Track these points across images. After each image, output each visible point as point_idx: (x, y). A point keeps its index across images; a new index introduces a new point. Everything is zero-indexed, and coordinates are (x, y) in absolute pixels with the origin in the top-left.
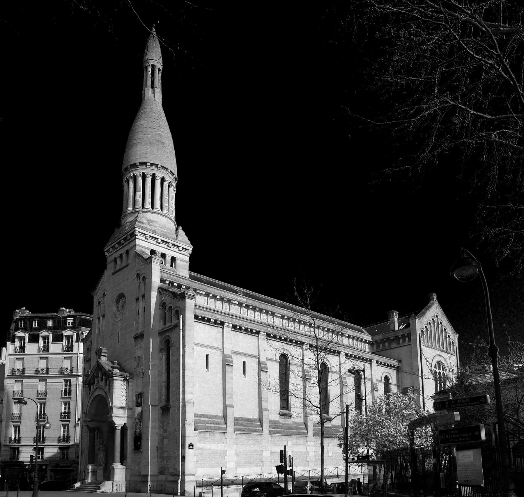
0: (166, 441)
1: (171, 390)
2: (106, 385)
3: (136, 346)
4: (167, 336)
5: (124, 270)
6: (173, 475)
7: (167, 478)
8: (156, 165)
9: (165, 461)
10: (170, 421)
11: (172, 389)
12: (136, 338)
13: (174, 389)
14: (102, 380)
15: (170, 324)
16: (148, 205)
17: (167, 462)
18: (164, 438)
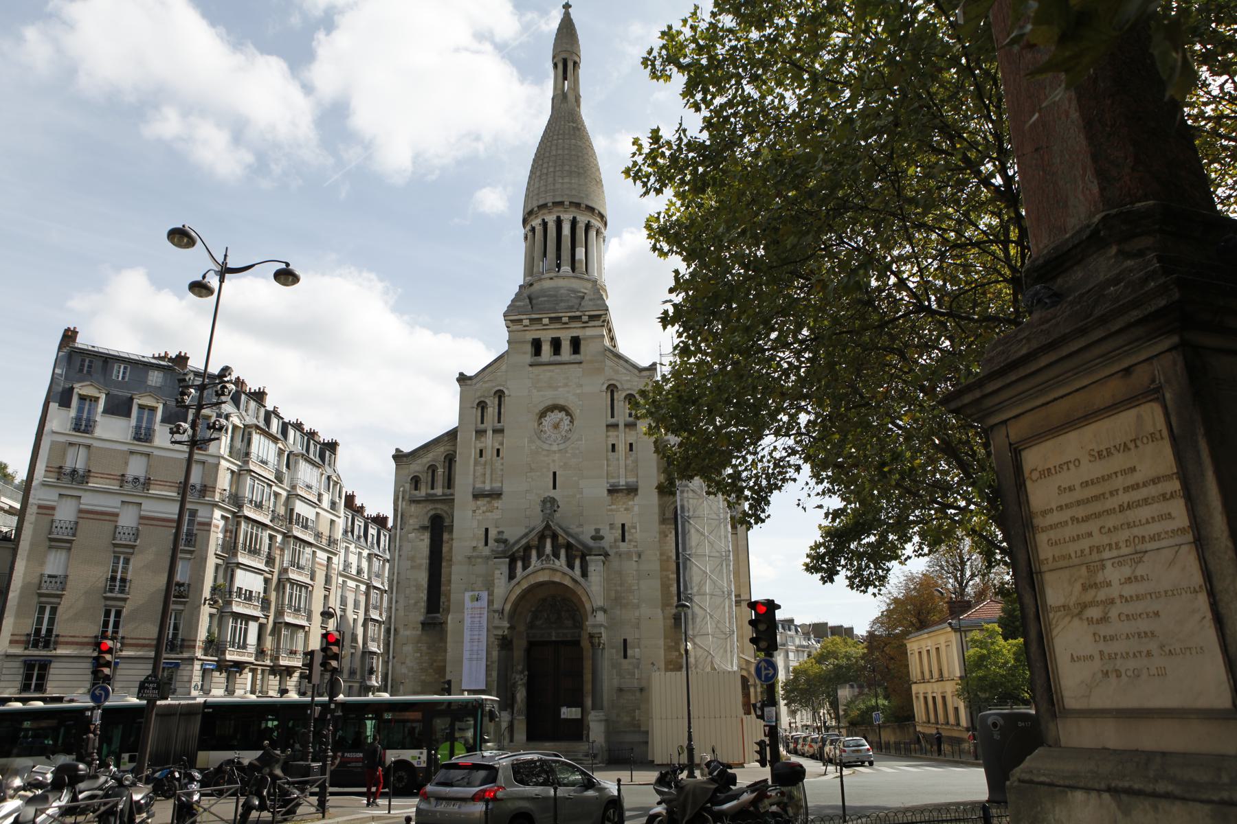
3: (612, 504)
8: (561, 203)
14: (557, 556)
16: (566, 268)
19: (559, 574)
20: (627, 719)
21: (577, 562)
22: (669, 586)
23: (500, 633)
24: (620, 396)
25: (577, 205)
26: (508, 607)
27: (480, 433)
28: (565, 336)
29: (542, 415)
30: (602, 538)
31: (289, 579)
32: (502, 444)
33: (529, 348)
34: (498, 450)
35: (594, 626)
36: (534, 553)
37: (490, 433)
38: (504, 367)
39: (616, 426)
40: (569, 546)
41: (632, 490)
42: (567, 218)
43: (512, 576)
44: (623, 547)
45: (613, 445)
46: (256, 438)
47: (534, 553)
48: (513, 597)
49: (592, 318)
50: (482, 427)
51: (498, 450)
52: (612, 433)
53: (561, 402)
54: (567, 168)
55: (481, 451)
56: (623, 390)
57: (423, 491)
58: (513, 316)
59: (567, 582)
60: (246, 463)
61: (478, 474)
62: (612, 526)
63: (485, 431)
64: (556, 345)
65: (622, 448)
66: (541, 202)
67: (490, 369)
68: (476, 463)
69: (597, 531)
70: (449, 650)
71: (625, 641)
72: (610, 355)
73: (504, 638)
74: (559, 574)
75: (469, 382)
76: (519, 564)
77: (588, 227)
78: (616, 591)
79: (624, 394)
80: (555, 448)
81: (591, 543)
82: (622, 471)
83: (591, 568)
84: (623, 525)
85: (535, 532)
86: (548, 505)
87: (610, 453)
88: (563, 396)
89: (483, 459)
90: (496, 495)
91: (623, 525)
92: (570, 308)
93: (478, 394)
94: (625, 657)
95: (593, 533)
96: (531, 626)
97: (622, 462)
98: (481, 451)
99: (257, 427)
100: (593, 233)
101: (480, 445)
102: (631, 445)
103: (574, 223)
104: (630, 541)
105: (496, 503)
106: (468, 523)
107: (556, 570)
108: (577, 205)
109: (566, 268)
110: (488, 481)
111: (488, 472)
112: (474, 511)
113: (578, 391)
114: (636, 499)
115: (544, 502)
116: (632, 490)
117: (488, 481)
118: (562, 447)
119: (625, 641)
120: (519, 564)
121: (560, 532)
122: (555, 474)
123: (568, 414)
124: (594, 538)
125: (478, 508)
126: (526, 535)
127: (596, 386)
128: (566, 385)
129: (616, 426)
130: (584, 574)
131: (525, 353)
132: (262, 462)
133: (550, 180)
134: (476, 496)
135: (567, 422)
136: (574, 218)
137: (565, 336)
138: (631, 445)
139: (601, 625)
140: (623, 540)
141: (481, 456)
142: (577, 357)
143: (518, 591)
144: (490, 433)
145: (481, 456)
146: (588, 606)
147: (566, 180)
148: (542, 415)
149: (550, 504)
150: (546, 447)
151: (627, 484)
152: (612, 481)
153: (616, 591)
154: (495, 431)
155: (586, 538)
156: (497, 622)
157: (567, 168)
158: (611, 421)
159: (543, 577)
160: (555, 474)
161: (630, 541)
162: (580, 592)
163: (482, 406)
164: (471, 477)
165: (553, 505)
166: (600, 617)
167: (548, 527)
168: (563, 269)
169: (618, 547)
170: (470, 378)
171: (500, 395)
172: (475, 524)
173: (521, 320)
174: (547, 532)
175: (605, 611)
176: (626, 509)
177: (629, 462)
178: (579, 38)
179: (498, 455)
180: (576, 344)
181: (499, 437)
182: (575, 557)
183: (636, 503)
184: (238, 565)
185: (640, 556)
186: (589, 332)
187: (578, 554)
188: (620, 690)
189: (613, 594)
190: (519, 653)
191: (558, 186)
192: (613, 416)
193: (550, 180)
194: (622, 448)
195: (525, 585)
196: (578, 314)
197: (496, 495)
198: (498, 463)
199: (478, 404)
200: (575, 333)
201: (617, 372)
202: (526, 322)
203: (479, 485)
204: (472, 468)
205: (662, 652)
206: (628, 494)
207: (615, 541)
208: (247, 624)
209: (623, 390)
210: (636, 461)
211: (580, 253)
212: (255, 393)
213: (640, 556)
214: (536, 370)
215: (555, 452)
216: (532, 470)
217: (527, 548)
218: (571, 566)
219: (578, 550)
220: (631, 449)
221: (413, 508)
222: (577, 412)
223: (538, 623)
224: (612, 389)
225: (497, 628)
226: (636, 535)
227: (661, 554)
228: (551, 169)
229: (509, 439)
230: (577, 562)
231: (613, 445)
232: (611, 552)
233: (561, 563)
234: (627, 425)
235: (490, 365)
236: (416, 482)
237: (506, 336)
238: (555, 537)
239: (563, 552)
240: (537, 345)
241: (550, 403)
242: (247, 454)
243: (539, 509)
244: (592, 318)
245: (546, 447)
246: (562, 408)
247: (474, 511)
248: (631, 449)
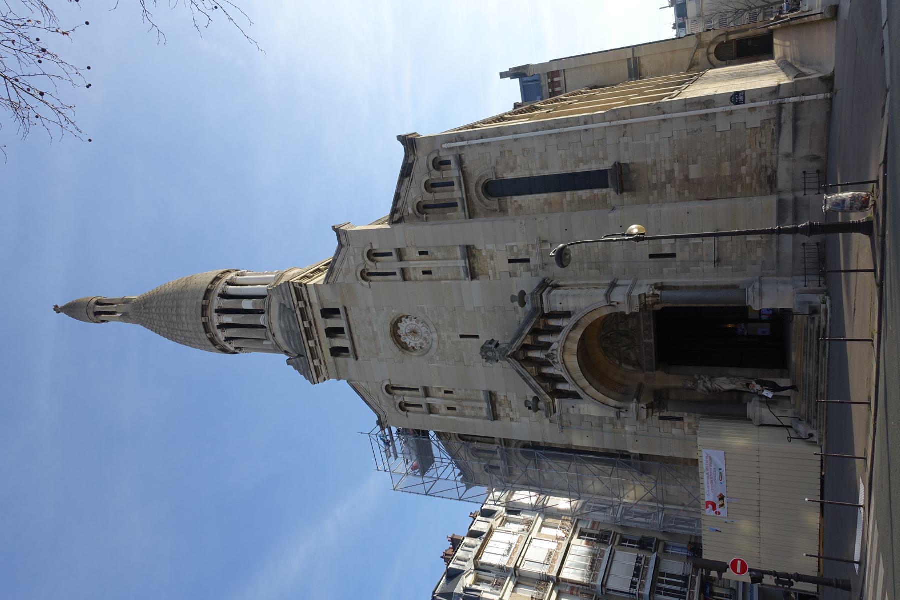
0: (695, 172)
1: (583, 168)
2: (558, 330)
3: (487, 274)
4: (477, 192)
5: (352, 323)
6: (780, 131)
7: (788, 156)
9: (744, 170)
10: (650, 161)
11: (580, 161)
12: (472, 274)
13: (580, 155)
14: (548, 346)
15: (456, 187)
17: (744, 163)
18: (687, 179)
19: (569, 344)
20: (760, 252)
21: (553, 323)
22: (581, 201)
23: (644, 412)
24: (372, 267)
25: (204, 309)
26: (612, 402)
27: (431, 410)
28: (323, 324)
29: (404, 347)
30: (523, 294)
31: (622, 517)
32: (440, 389)
33: (341, 360)
34: (446, 392)
35: (630, 304)
36: (546, 371)
37: (429, 400)
38: (364, 385)
39: (403, 271)
40: (535, 332)
41: (469, 252)
42: (217, 320)
43: (575, 396)
44: (535, 261)
45: (425, 273)
46: (486, 559)
47: (546, 371)
48: (600, 396)
49: (300, 297)
50: (425, 408)
51: (446, 392)
52: (412, 275)
53: (388, 328)
54: (174, 319)
55: (449, 409)
56: (365, 264)
57: (500, 463)
58: (315, 375)
59: (578, 335)
60: (508, 569)
61: (473, 413)
62: (512, 275)
63: (429, 405)
64: (333, 333)
65: (426, 264)
66: (209, 343)
67: (367, 398)
68: (462, 415)
69: (513, 299)
70: (671, 454)
71: (651, 256)
72: (332, 278)
73: (650, 407)
74: (569, 344)
75: (383, 419)
76: (560, 387)
77: (224, 296)
78: (590, 268)
79: (369, 262)
80: (435, 336)
81: (528, 307)
82: (450, 263)
83: (558, 307)
84: (510, 261)
85: (521, 369)
86: (490, 354)
87: (434, 276)
88: (382, 329)
89: (457, 407)
90: (492, 397)
91: (510, 261)
92: (295, 320)
93: (393, 409)
94: (673, 256)
95: (516, 304)
96: (638, 365)
97: (441, 264)
98: (449, 409)
99: (477, 557)
100: (231, 290)
101: (444, 411)
102: (421, 253)
103: (221, 311)
104: (528, 253)
105: (501, 396)
106: (524, 425)
107: (564, 347)
108: (204, 309)
109: (262, 320)
110: (479, 405)
111: (469, 404)
112: (512, 420)
113: (374, 311)
114: (480, 246)
115: (488, 359)
116: (469, 252)
117: (479, 405)
118: (433, 330)
119: (651, 256)
120: (560, 387)
121: (518, 343)
122: (462, 337)
123: (400, 320)
124: (523, 304)
125: (508, 415)
126: (525, 379)
127: (365, 293)
128: (370, 324)
129: (403, 271)
130: (567, 315)
131: (346, 364)
132: (509, 551)
133: (187, 334)
134: (495, 417)
135: (408, 320)
136: (217, 311)
137: (323, 324)
138: (421, 253)
139: (629, 296)
140: (528, 261)
141: (455, 409)
142: (342, 310)
143: (592, 390)
144: (429, 400)
145: (455, 409)
146: (606, 312)
147: (184, 320)
148: (404, 347)
149: (491, 351)
150: (435, 345)
151: (464, 258)
152: (463, 275)
153: (590, 268)
154: (427, 395)
155: (521, 314)
156: (632, 415)
157: (174, 319)
158: (399, 276)
159: (573, 361)
160: (462, 337)
161: (528, 253)
162: (588, 321)
163: (404, 407)
164: (477, 421)
165: (490, 350)
166: (619, 296)
167: (514, 356)
168: (262, 323)
169: (536, 266)
170: (379, 417)
171: (390, 389)
172: (525, 419)
173: (315, 367)
174: (521, 357)
175: (613, 285)
176: (492, 258)
177: (440, 255)
178: (71, 301)
179: (451, 392)
180: (329, 313)
181: (432, 392)
182: (546, 325)
183: (484, 247)
184: (603, 585)
185: (545, 241)
186: (315, 300)
187: (542, 323)
188: (718, 261)
189: (594, 272)
190: (672, 380)
191: (191, 328)
192: (394, 274)
193: (187, 334)
194: (426, 264)
195: (584, 383)
196: (298, 312)
197: (492, 397)
198: (459, 394)
199: (403, 410)
200: (318, 315)
201: (348, 271)
202: (317, 362)
203: (485, 413)
204: (467, 420)
205: (667, 209)
206: (474, 256)
207: (530, 270)
208: (663, 574)
209: (365, 264)
210: (438, 248)
211: (247, 305)
212: (453, 544)
213: (545, 241)
214: (360, 353)
215: (440, 336)
216: (461, 360)
217: (543, 378)
218: (558, 330)
219: (538, 323)
220: (426, 253)
221: (518, 473)
222: (396, 313)
223: (633, 357)
224: (366, 276)
225: (638, 416)
226: (520, 246)
227: (543, 212)
228: (179, 333)
229: (435, 385)
230: (553, 323)
231: (425, 273)
232: (543, 275)
233: (556, 341)
234: (401, 259)
235: (363, 398)
236: (491, 469)
237: (333, 382)
238: (525, 348)
239: (542, 339)
240: (337, 352)
241: (390, 342)
242: (501, 568)
243: (495, 364)
244: (300, 297)
245: (435, 345)
246: (395, 327)
247: (512, 420)
248: (426, 253)
